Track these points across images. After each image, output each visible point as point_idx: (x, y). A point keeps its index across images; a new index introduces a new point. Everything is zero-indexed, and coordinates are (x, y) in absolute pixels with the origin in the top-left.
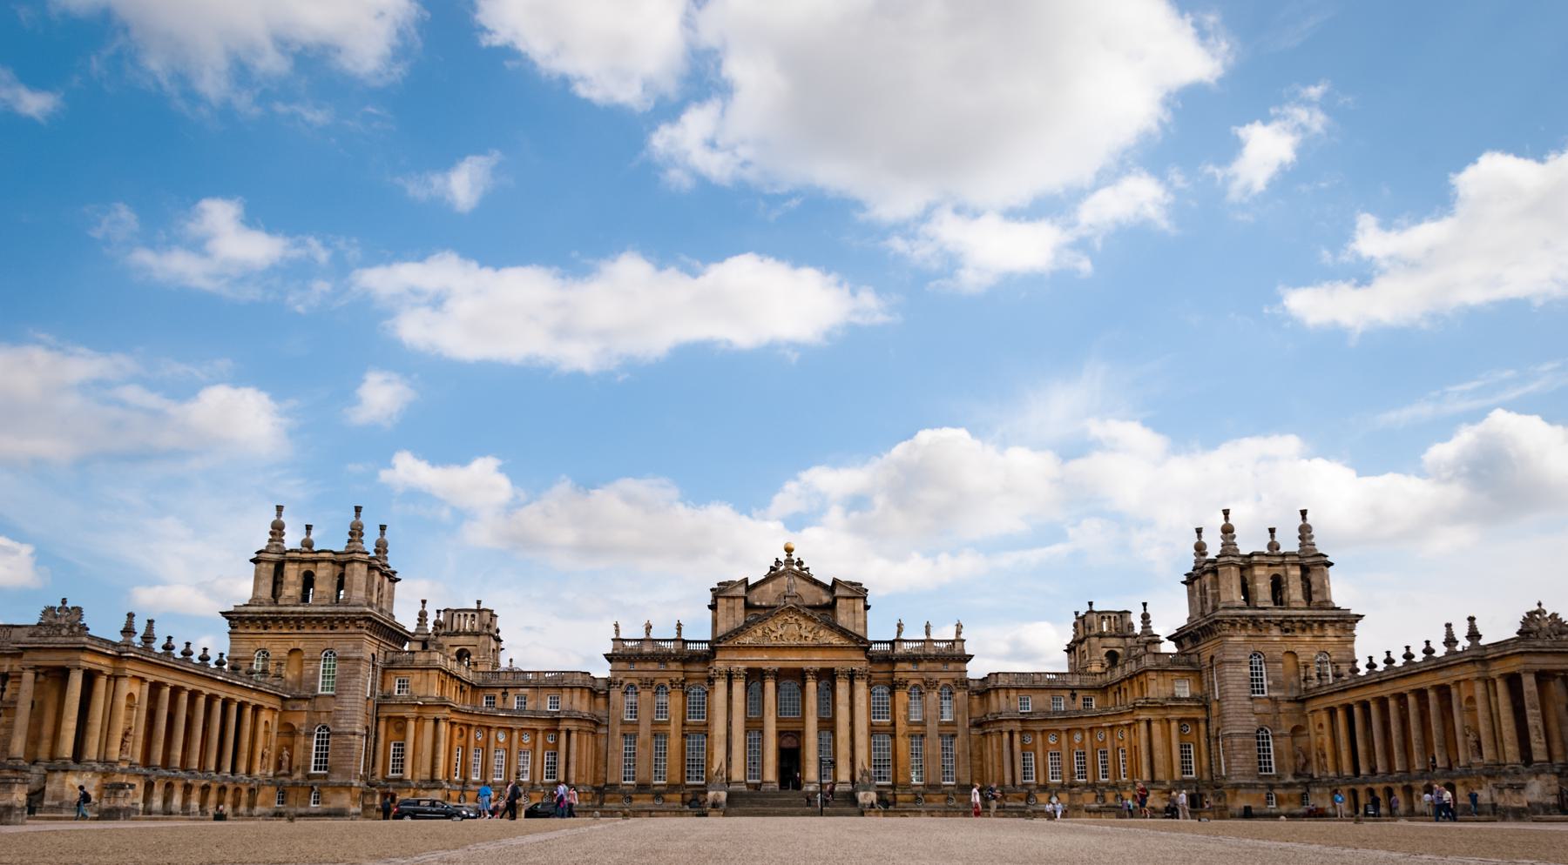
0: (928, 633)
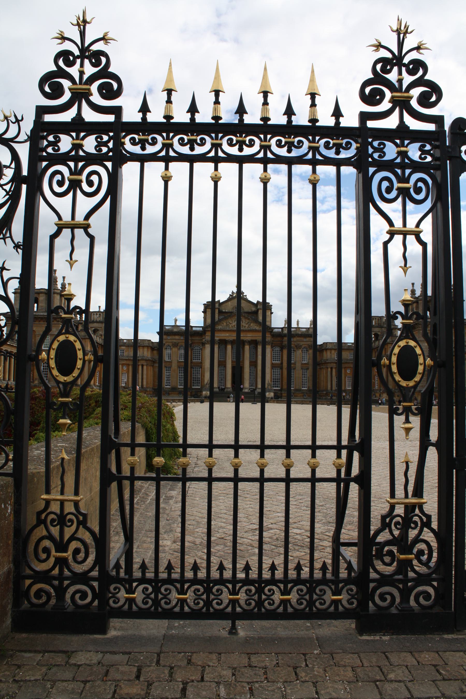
0: (298, 324)
